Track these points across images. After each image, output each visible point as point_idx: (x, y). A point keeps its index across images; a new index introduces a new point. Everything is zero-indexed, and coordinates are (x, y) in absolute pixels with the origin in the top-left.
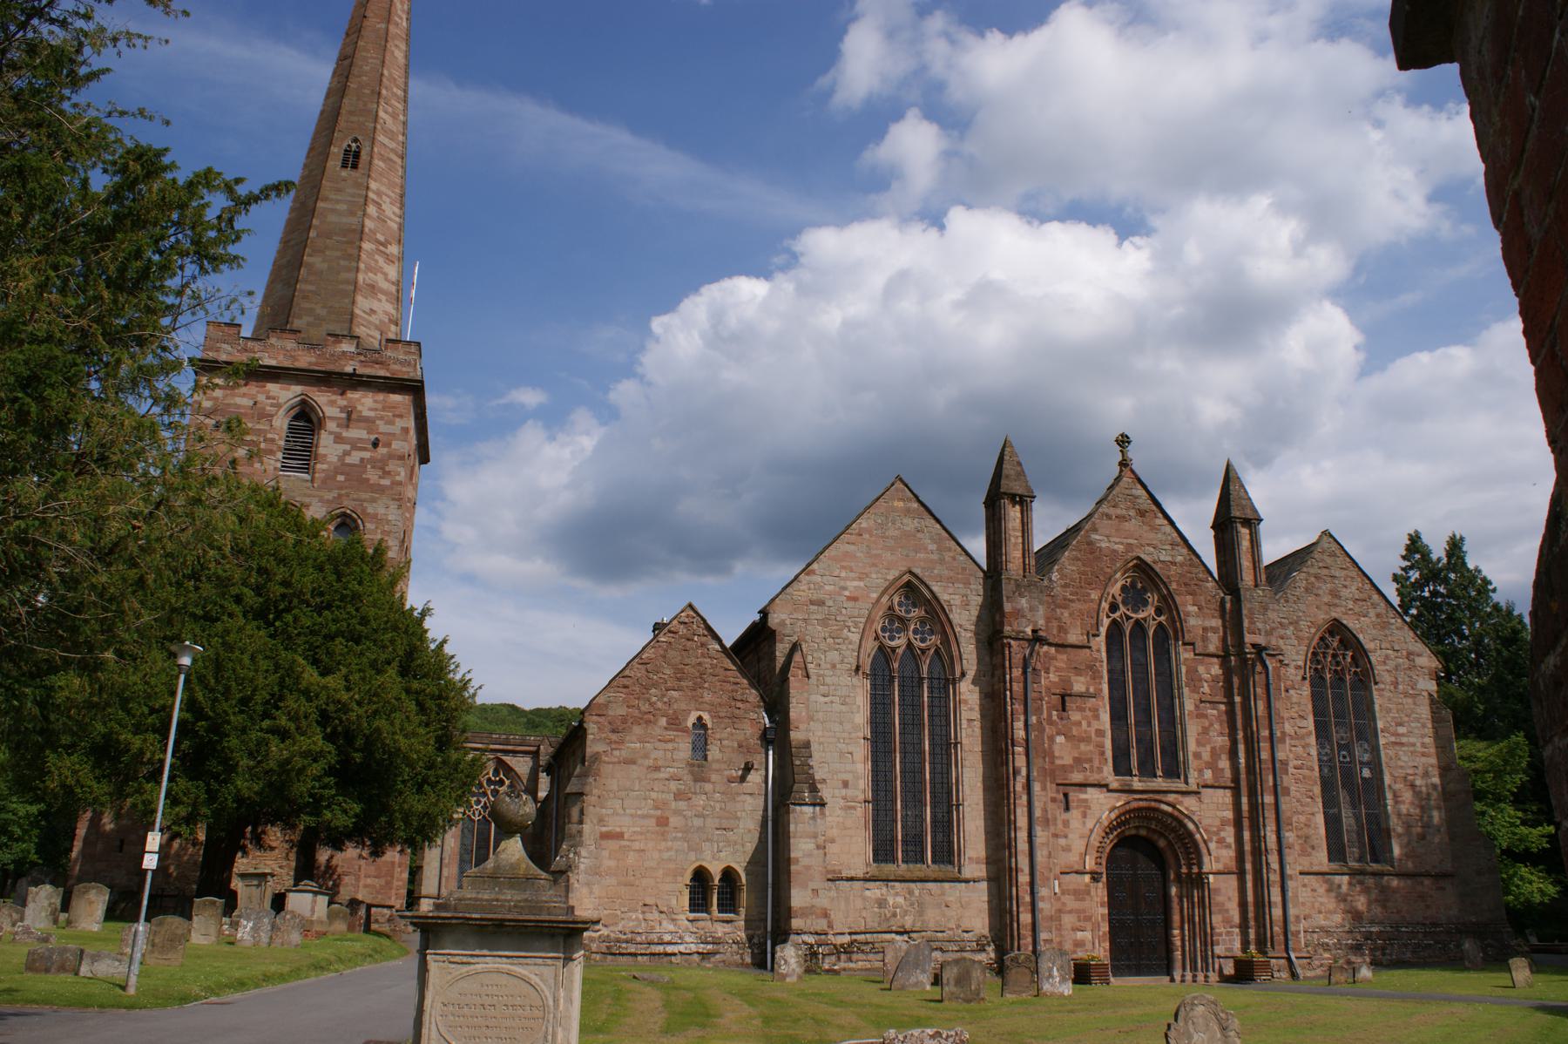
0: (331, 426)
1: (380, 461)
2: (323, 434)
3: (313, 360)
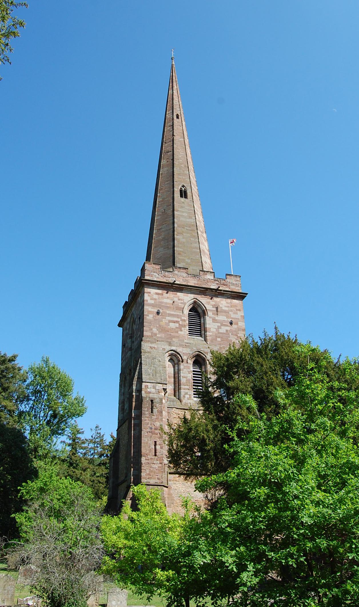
0: (210, 314)
1: (235, 331)
2: (207, 318)
3: (196, 282)
